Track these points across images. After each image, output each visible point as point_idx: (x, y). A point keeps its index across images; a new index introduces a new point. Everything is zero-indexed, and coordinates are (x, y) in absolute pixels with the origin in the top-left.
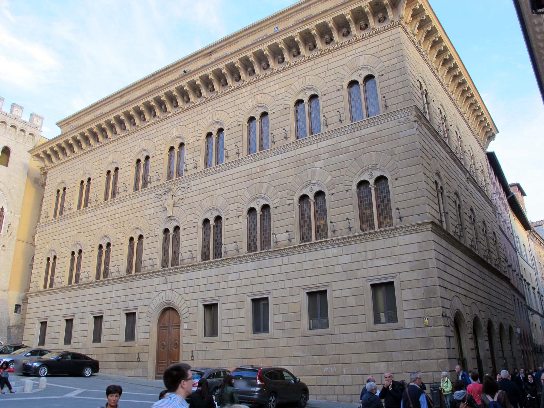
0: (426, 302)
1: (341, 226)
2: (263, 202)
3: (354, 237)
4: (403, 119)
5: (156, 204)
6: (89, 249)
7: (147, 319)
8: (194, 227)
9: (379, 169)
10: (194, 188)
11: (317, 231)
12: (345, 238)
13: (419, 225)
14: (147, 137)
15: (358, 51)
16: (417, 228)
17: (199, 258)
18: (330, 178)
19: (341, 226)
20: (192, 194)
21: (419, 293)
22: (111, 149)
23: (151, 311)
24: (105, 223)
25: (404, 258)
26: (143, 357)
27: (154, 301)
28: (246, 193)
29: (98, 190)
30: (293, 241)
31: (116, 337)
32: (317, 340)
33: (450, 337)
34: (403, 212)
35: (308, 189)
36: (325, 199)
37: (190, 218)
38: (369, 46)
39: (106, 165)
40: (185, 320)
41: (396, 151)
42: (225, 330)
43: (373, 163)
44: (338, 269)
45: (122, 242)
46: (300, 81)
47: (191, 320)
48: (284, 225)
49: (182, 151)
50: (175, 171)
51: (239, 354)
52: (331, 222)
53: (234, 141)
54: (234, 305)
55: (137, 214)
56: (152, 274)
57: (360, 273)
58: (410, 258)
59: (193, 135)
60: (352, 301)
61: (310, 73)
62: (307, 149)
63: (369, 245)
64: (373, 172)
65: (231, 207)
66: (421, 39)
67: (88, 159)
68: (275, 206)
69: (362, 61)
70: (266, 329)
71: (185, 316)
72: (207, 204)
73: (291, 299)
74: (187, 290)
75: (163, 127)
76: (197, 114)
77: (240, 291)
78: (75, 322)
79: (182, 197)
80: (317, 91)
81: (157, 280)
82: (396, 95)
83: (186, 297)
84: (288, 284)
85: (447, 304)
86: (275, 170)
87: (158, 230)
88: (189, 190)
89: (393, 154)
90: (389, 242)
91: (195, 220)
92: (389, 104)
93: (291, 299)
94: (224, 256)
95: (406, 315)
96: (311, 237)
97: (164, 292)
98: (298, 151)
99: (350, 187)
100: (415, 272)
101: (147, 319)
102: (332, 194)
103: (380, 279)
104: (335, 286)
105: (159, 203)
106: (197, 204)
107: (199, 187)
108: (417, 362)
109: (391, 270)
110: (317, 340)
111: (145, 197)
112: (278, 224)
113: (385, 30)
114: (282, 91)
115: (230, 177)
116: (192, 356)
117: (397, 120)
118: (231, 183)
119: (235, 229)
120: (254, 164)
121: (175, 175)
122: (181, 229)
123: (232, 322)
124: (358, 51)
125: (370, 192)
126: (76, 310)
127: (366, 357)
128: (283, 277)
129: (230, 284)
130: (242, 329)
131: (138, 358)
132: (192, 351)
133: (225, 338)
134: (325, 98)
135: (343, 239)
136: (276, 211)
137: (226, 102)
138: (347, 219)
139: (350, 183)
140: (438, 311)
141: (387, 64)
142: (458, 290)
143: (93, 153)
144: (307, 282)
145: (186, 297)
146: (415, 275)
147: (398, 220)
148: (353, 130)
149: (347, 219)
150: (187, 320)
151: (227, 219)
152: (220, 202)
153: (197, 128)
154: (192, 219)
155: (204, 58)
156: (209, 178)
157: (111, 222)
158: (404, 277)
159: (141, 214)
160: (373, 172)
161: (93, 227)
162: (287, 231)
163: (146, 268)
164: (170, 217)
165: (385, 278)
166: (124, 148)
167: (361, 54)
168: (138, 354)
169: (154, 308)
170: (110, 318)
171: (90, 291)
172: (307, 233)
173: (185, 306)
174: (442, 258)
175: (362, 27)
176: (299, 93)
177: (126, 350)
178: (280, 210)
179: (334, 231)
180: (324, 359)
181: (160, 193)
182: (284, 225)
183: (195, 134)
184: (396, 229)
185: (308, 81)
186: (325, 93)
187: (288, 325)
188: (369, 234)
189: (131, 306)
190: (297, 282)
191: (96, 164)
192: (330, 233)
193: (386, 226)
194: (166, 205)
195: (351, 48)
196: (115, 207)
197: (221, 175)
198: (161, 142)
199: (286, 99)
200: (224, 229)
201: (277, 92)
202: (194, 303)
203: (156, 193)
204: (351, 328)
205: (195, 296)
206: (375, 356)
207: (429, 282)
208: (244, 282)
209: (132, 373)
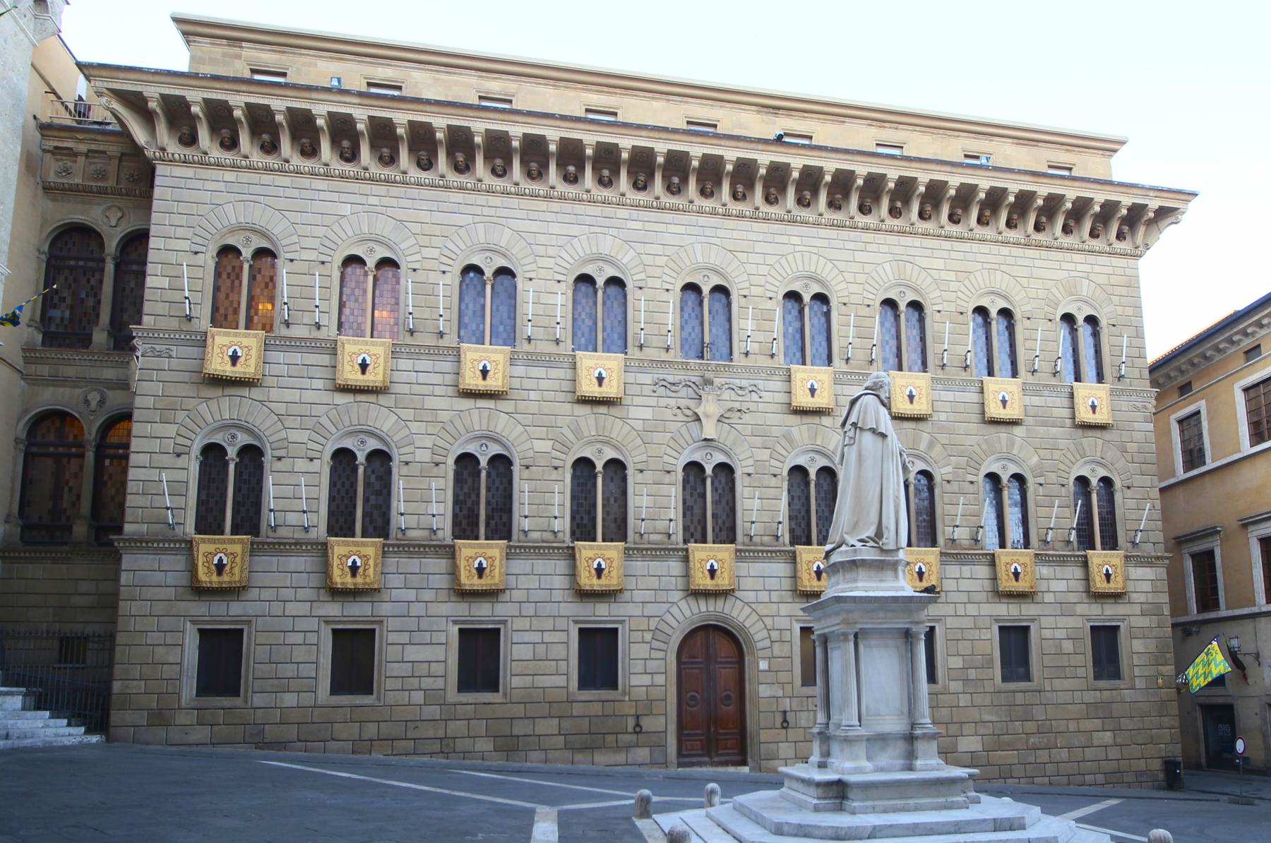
3: (1074, 556)
5: (664, 402)
6: (424, 456)
7: (656, 644)
10: (767, 397)
12: (1063, 556)
13: (1158, 558)
14: (612, 231)
15: (1080, 267)
18: (1035, 459)
22: (478, 210)
26: (647, 723)
32: (1019, 698)
37: (765, 455)
38: (1096, 269)
40: (760, 654)
41: (1132, 447)
45: (557, 463)
47: (776, 653)
58: (1142, 598)
59: (755, 280)
60: (1068, 646)
67: (373, 200)
69: (1085, 289)
74: (764, 596)
75: (661, 227)
76: (761, 237)
79: (737, 405)
84: (972, 609)
88: (755, 397)
91: (773, 462)
100: (1147, 618)
103: (1104, 620)
104: (1046, 622)
106: (776, 431)
110: (1019, 698)
114: (952, 276)
124: (1080, 267)
127: (1087, 725)
131: (638, 725)
132: (785, 712)
135: (1060, 556)
137: (835, 243)
141: (1120, 310)
143: (395, 191)
146: (1144, 622)
150: (767, 653)
153: (763, 270)
154: (766, 457)
155: (759, 112)
166: (533, 226)
167: (1084, 275)
168: (638, 717)
176: (982, 295)
178: (955, 487)
180: (1031, 727)
181: (671, 379)
183: (761, 281)
187: (972, 674)
191: (416, 228)
194: (700, 411)
195: (1068, 255)
198: (661, 261)
199: (960, 294)
202: (783, 623)
203: (661, 377)
204: (1067, 684)
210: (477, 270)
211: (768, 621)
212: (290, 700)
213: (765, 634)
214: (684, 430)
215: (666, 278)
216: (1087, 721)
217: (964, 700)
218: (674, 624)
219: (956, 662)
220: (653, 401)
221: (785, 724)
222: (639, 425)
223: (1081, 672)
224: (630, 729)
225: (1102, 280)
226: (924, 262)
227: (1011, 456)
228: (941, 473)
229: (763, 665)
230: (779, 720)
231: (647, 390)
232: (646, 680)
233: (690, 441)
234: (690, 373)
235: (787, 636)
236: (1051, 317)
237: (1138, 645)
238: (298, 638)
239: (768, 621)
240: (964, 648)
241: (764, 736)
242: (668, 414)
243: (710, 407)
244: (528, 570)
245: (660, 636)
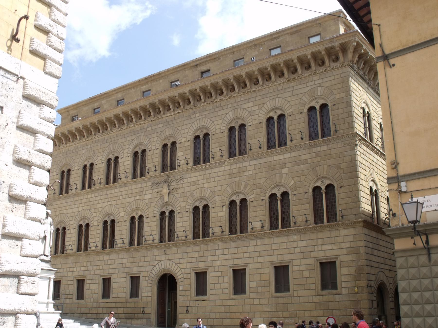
0: (357, 277)
1: (301, 219)
2: (242, 197)
4: (347, 142)
5: (154, 191)
8: (187, 212)
9: (328, 178)
11: (283, 221)
15: (316, 82)
16: (352, 225)
17: (190, 236)
18: (292, 182)
19: (301, 219)
20: (184, 185)
21: (353, 270)
23: (153, 276)
24: (109, 203)
25: (343, 245)
27: (155, 268)
28: (228, 189)
29: (99, 173)
30: (265, 228)
31: (124, 295)
32: (281, 300)
33: (372, 301)
34: (344, 212)
35: (276, 189)
36: (289, 197)
39: (107, 153)
41: (342, 166)
42: (213, 292)
43: (325, 173)
44: (297, 250)
46: (271, 101)
47: (186, 283)
48: (258, 216)
49: (174, 148)
50: (169, 165)
51: (223, 309)
52: (293, 216)
53: (218, 145)
54: (219, 274)
55: (137, 198)
56: (152, 246)
57: (313, 254)
58: (348, 245)
60: (306, 274)
61: (279, 96)
62: (276, 158)
63: (320, 235)
64: (324, 180)
65: (217, 198)
66: (366, 71)
68: (251, 200)
69: (320, 91)
70: (243, 291)
71: (180, 280)
72: (197, 194)
73: (262, 271)
77: (224, 263)
78: (87, 282)
79: (175, 187)
80: (284, 111)
81: (156, 252)
82: (343, 122)
83: (181, 266)
84: (261, 259)
85: (373, 278)
86: (251, 172)
88: (182, 182)
89: (339, 168)
90: (334, 234)
92: (338, 129)
93: (262, 271)
94: (211, 237)
95: (344, 285)
96: (278, 225)
98: (270, 159)
99: (307, 191)
100: (350, 256)
102: (295, 195)
103: (327, 259)
104: (295, 262)
105: (156, 190)
107: (190, 180)
108: (349, 317)
109: (335, 253)
110: (281, 300)
111: (143, 184)
112: (254, 214)
113: (337, 68)
114: (256, 108)
115: (215, 175)
116: (187, 310)
117: (343, 143)
118: (216, 179)
119: (219, 216)
120: (234, 166)
121: (169, 168)
122: (176, 212)
123: (217, 286)
125: (322, 195)
126: (86, 273)
128: (257, 254)
129: (216, 258)
130: (226, 291)
131: (143, 311)
132: (187, 307)
133: (212, 297)
134: (290, 118)
136: (252, 204)
138: (305, 215)
139: (307, 188)
140: (363, 283)
142: (383, 266)
144: (274, 258)
145: (181, 266)
146: (349, 258)
147: (341, 218)
148: (311, 147)
149: (305, 215)
151: (214, 208)
152: (207, 194)
156: (198, 174)
157: (114, 203)
158: (343, 258)
159: (141, 198)
160: (324, 180)
162: (260, 221)
163: (147, 242)
165: (330, 259)
168: (143, 308)
169: (155, 273)
170: (118, 280)
171: (97, 258)
172: (275, 222)
173: (180, 272)
174: (370, 245)
175: (320, 64)
177: (132, 305)
178: (255, 203)
179: (295, 223)
180: (286, 314)
181: (156, 182)
182: (258, 216)
184: (339, 224)
185: (278, 102)
186: (291, 114)
187: (260, 289)
188: (320, 226)
189: (135, 271)
192: (292, 224)
193: (332, 221)
196: (117, 190)
197: (207, 172)
200: (212, 215)
201: (253, 109)
202: (188, 271)
205: (189, 265)
206: (321, 312)
207: (359, 263)
208: (227, 257)
209: (138, 322)
212: (68, 301)
213: (181, 276)
215: (157, 145)
216: (315, 312)
217: (256, 302)
219: (253, 284)
220: (151, 192)
222: (147, 201)
223: (313, 286)
224: (141, 312)
225: (328, 84)
226: (245, 106)
227: (281, 184)
228: (249, 198)
230: (186, 310)
231: (150, 188)
232: (146, 294)
235: (189, 276)
236: (302, 111)
237: (344, 271)
238: (69, 283)
239: (183, 270)
240: (257, 278)
244: (117, 258)
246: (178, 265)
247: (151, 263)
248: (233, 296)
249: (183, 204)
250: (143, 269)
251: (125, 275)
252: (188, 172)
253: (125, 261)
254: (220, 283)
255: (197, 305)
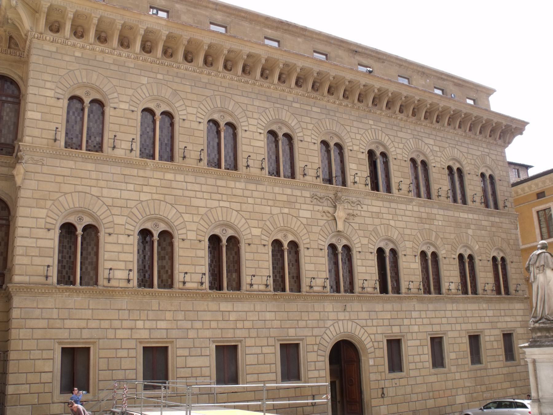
5: (317, 208)
7: (320, 352)
47: (377, 355)
70: (442, 365)
77: (422, 329)
81: (329, 306)
84: (458, 327)
87: (323, 243)
97: (340, 323)
101: (320, 352)
107: (371, 209)
129: (413, 321)
132: (383, 388)
133: (412, 373)
144: (469, 327)
152: (395, 235)
154: (367, 243)
157: (236, 206)
161: (195, 202)
164: (339, 231)
189: (291, 335)
190: (464, 327)
210: (80, 100)
211: (372, 337)
214: (327, 225)
217: (458, 376)
218: (328, 340)
219: (453, 356)
220: (311, 208)
221: (383, 395)
222: (304, 221)
229: (371, 362)
233: (331, 232)
234: (328, 192)
241: (374, 402)
242: (319, 216)
243: (341, 214)
244: (252, 309)
245: (322, 348)
246: (365, 328)
247: (321, 324)
248: (433, 371)
249: (365, 241)
250: (307, 332)
251: (271, 341)
252: (368, 197)
253: (268, 316)
254: (417, 353)
255: (394, 385)
